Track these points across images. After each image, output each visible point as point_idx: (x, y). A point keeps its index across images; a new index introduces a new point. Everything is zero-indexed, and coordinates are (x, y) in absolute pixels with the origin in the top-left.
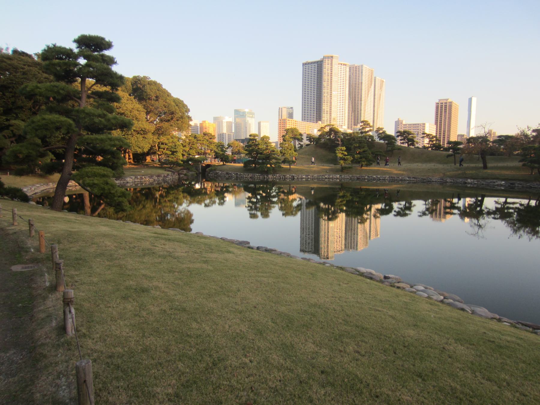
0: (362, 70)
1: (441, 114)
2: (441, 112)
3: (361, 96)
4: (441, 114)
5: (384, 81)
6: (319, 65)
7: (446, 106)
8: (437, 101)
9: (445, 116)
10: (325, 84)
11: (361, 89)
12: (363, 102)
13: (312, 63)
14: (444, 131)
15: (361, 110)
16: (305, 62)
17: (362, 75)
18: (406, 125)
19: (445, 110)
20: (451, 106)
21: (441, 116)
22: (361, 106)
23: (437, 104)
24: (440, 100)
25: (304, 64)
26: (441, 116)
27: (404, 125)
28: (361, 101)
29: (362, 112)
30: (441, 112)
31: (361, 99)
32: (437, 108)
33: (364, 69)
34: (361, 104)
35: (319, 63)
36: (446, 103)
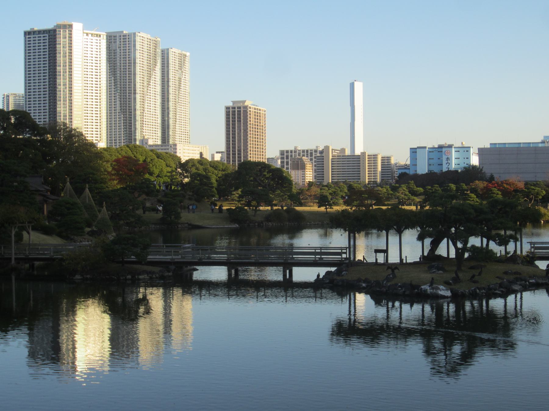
0: (135, 41)
1: (234, 125)
2: (234, 121)
3: (135, 85)
4: (234, 125)
5: (188, 54)
6: (51, 35)
7: (239, 112)
8: (231, 104)
9: (239, 127)
10: (60, 69)
11: (135, 74)
12: (138, 97)
13: (39, 32)
14: (239, 151)
15: (135, 110)
16: (28, 29)
17: (135, 50)
18: (152, 146)
19: (239, 118)
20: (246, 112)
21: (234, 128)
22: (135, 102)
23: (227, 108)
24: (234, 102)
26: (234, 128)
28: (135, 93)
29: (138, 113)
30: (234, 121)
31: (135, 90)
32: (228, 114)
33: (138, 39)
34: (135, 99)
35: (52, 33)
36: (239, 108)
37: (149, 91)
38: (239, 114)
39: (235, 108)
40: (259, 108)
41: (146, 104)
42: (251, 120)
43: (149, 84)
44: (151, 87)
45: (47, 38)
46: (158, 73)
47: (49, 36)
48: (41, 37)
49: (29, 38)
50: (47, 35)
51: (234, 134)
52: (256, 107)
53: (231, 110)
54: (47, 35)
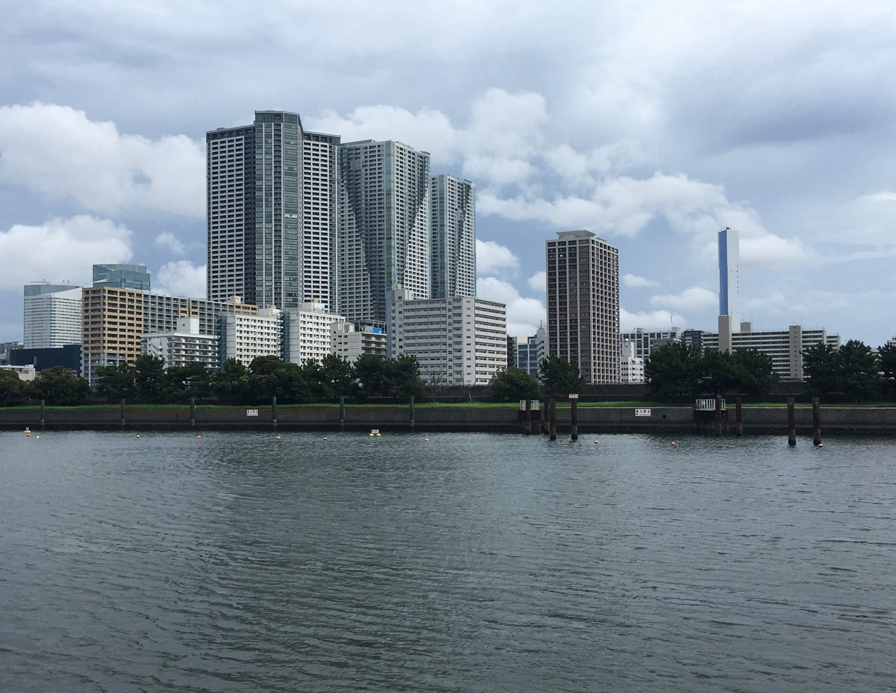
8: (556, 238)
14: (574, 321)
16: (214, 129)
20: (585, 250)
23: (551, 244)
24: (561, 234)
25: (211, 136)
27: (408, 303)
32: (551, 253)
37: (412, 236)
38: (573, 255)
39: (564, 243)
40: (608, 245)
41: (408, 257)
42: (594, 265)
43: (412, 226)
44: (416, 229)
45: (243, 142)
46: (427, 208)
47: (246, 139)
48: (233, 141)
49: (214, 143)
50: (243, 137)
51: (563, 291)
52: (604, 243)
53: (557, 247)
54: (243, 137)
